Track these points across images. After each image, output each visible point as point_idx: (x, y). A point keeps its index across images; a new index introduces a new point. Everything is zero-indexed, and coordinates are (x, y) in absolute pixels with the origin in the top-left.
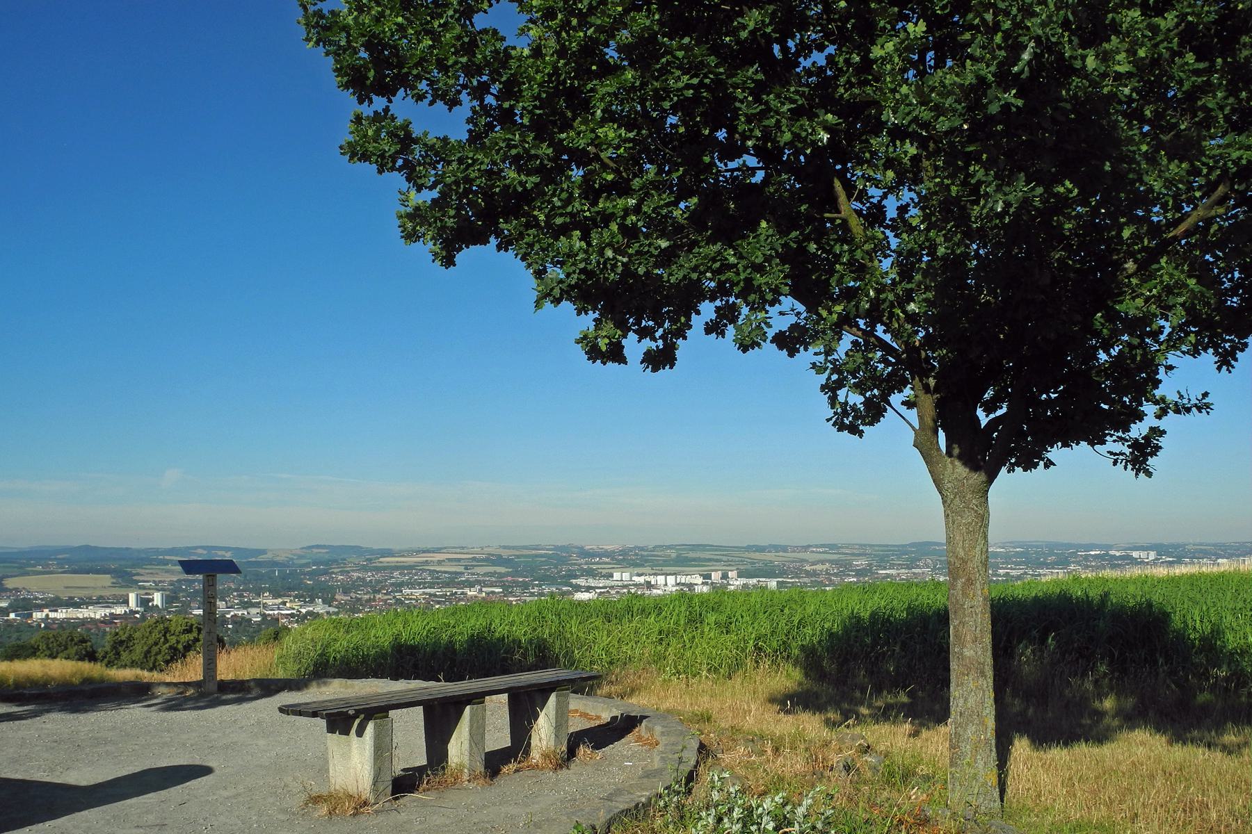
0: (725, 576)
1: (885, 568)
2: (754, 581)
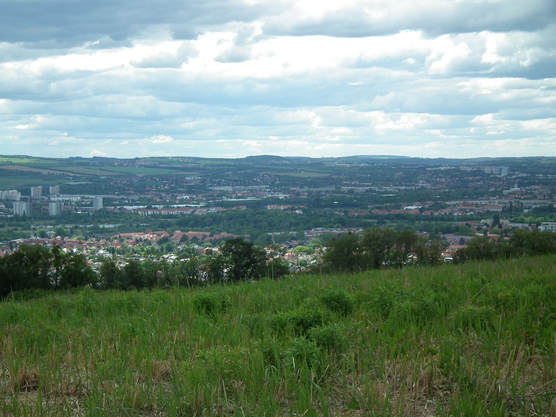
0: (46, 192)
1: (219, 184)
2: (76, 198)
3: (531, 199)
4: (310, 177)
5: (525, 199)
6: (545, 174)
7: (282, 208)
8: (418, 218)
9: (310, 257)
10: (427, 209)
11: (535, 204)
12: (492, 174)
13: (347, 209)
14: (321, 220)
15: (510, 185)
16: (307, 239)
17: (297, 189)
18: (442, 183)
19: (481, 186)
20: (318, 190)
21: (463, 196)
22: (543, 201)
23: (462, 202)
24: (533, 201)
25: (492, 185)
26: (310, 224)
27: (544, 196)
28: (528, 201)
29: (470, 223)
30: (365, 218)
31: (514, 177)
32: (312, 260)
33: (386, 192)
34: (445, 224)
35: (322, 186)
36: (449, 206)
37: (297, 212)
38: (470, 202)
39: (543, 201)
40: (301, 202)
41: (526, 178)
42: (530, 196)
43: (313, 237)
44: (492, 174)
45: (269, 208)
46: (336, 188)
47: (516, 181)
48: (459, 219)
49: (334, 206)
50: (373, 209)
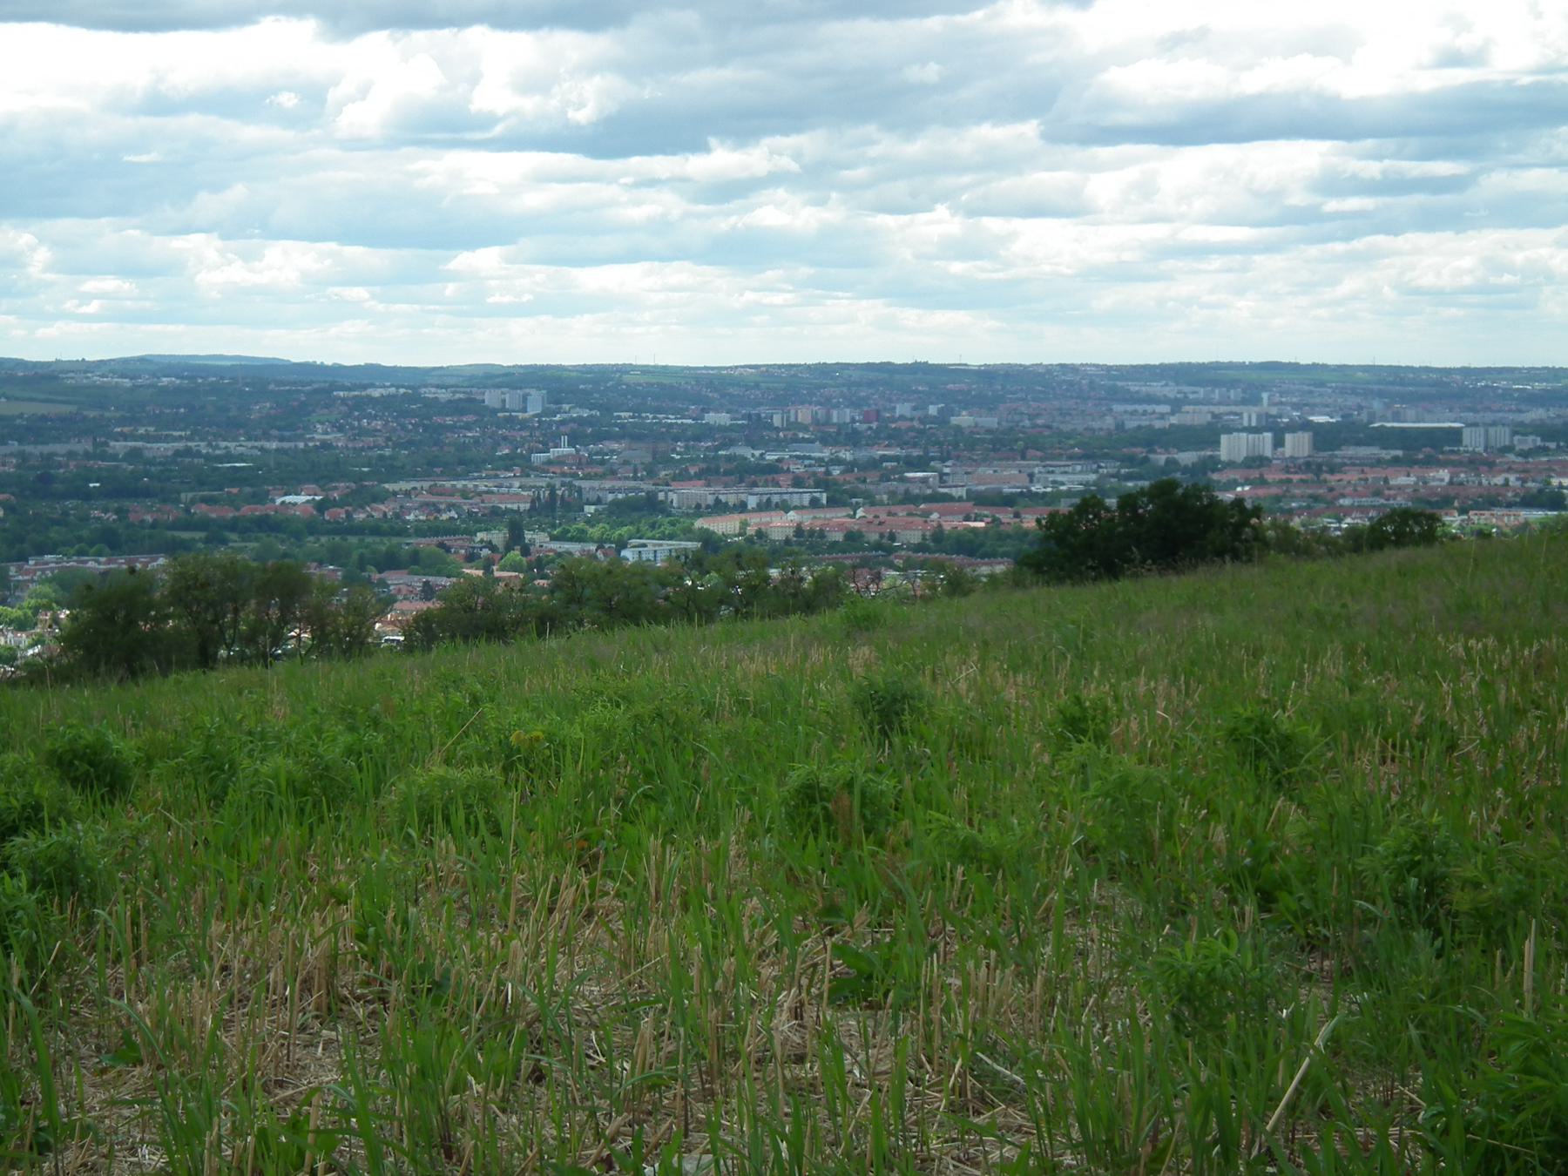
3: (602, 477)
4: (22, 414)
5: (587, 477)
6: (637, 410)
8: (312, 528)
9: (24, 638)
10: (335, 504)
11: (612, 491)
12: (503, 409)
13: (127, 504)
14: (55, 534)
15: (550, 440)
16: (16, 587)
18: (373, 432)
19: (476, 441)
20: (47, 449)
21: (430, 467)
22: (632, 484)
23: (426, 485)
24: (608, 484)
25: (505, 438)
26: (25, 545)
27: (635, 472)
28: (596, 484)
29: (448, 541)
30: (175, 526)
31: (558, 417)
32: (32, 646)
33: (229, 457)
34: (384, 544)
35: (57, 440)
36: (395, 494)
38: (448, 484)
39: (632, 484)
41: (589, 421)
42: (600, 470)
43: (32, 581)
44: (503, 409)
46: (95, 444)
47: (562, 429)
48: (420, 532)
49: (88, 496)
50: (193, 502)
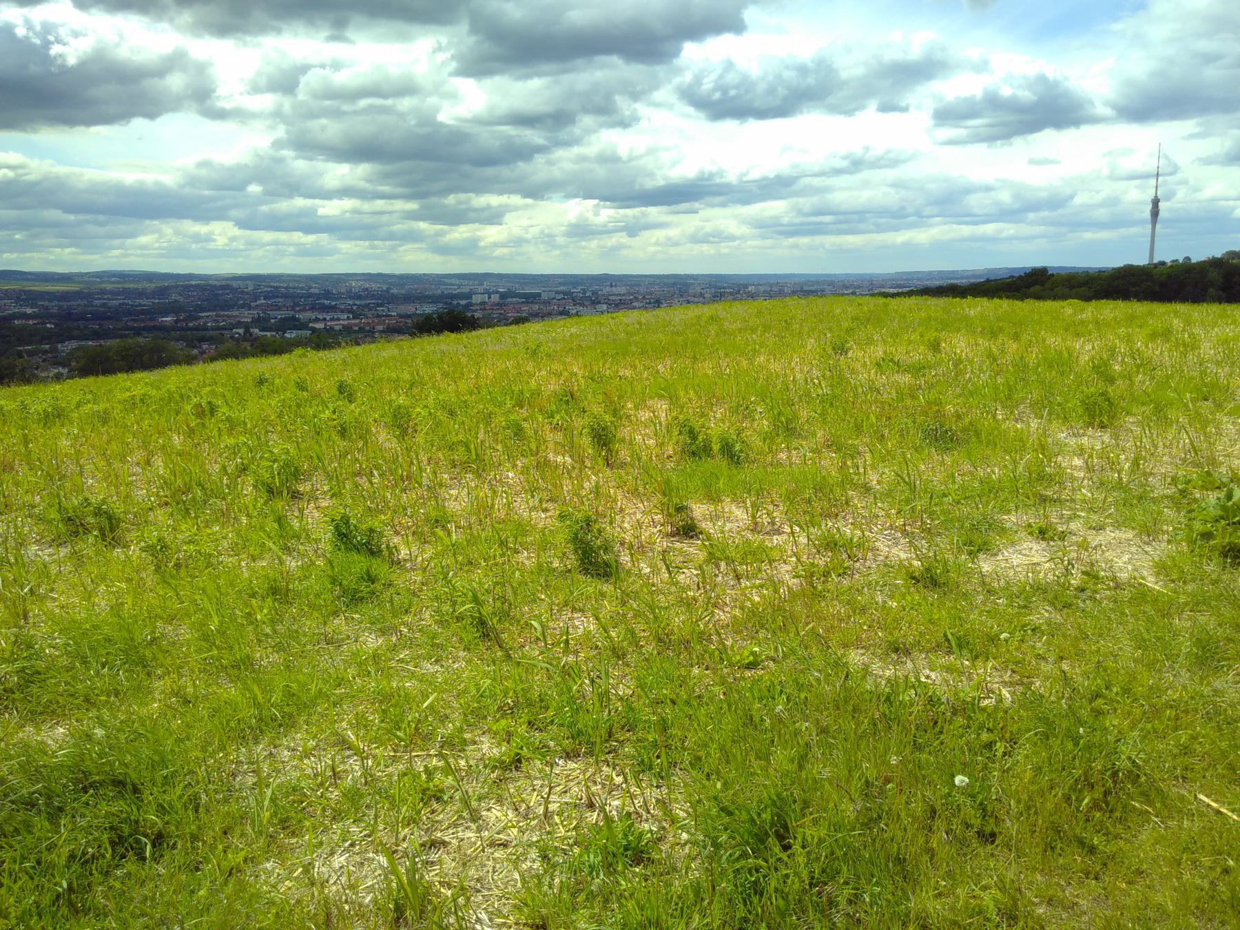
7: (31, 322)
8: (173, 329)
10: (183, 321)
14: (76, 333)
17: (46, 303)
18: (193, 296)
21: (215, 307)
33: (140, 305)
34: (202, 333)
35: (73, 300)
37: (48, 325)
40: (51, 316)
41: (270, 292)
45: (16, 322)
48: (213, 329)
49: (87, 320)
